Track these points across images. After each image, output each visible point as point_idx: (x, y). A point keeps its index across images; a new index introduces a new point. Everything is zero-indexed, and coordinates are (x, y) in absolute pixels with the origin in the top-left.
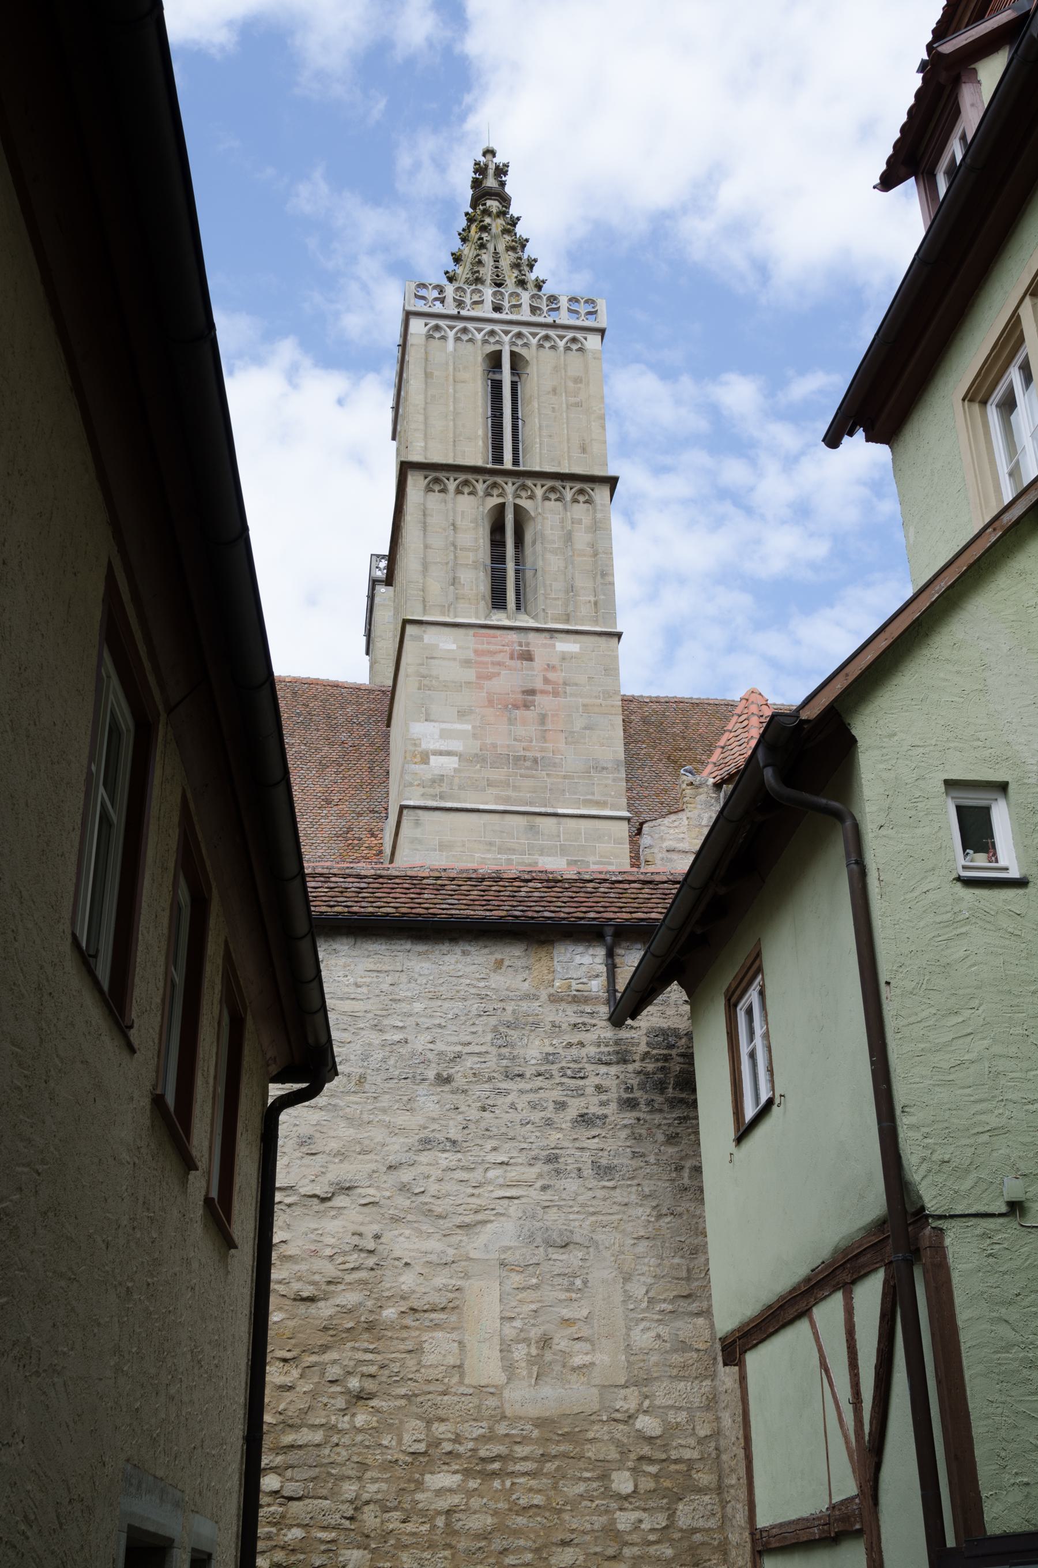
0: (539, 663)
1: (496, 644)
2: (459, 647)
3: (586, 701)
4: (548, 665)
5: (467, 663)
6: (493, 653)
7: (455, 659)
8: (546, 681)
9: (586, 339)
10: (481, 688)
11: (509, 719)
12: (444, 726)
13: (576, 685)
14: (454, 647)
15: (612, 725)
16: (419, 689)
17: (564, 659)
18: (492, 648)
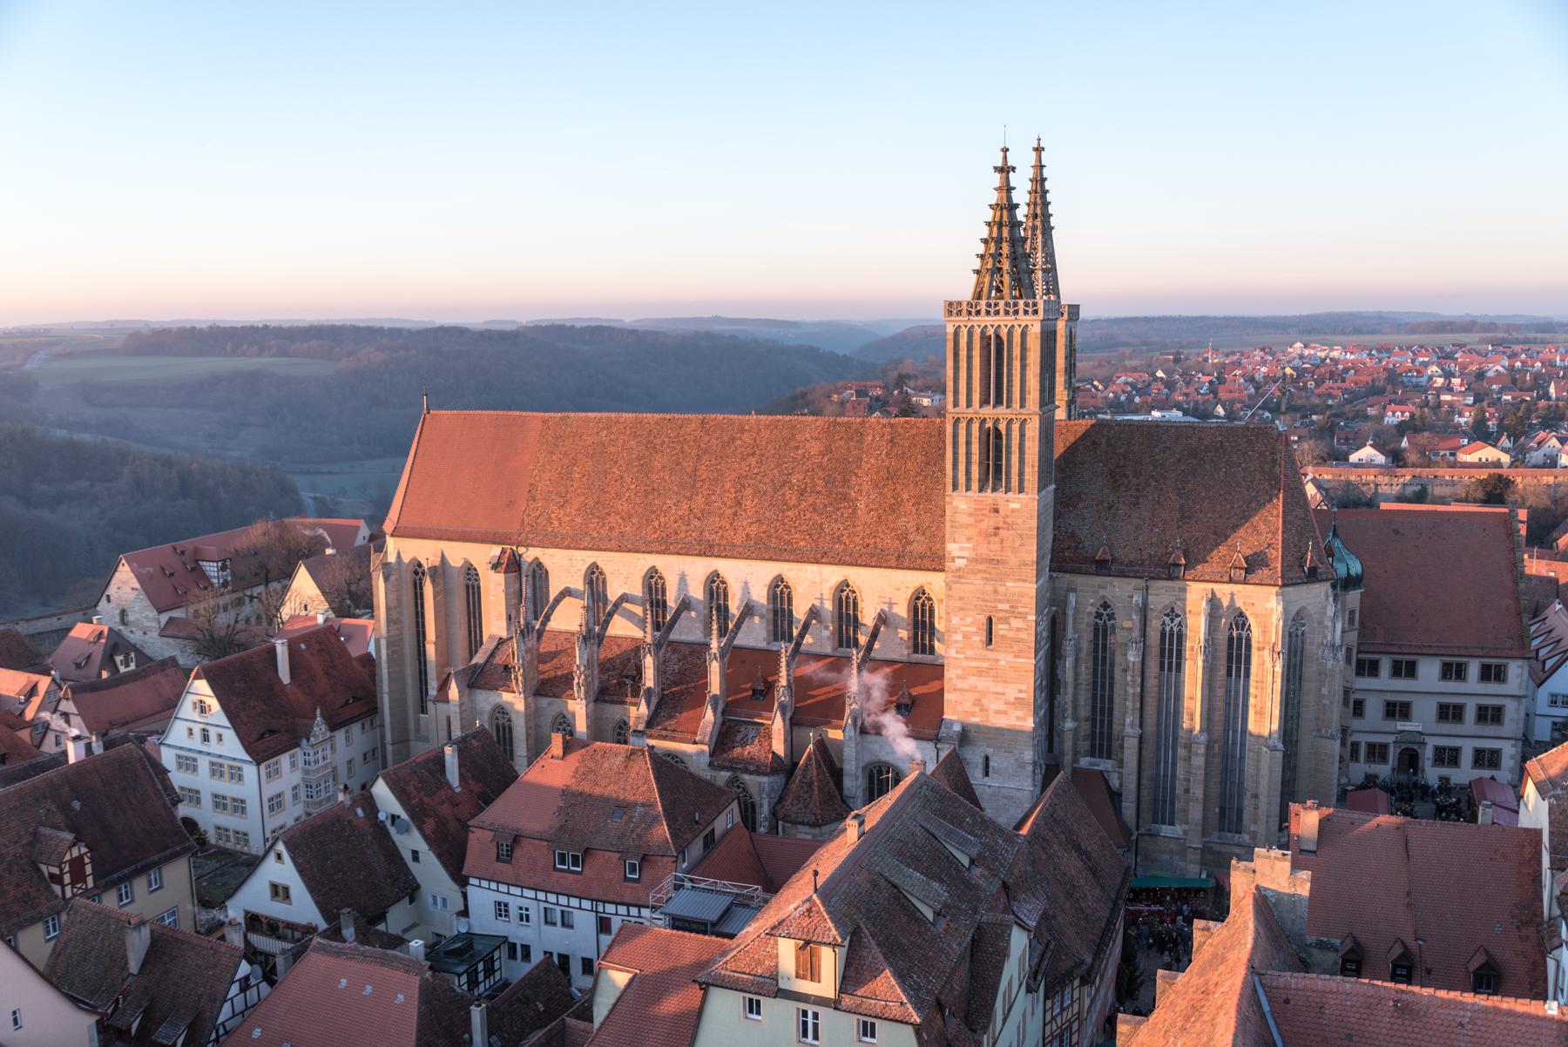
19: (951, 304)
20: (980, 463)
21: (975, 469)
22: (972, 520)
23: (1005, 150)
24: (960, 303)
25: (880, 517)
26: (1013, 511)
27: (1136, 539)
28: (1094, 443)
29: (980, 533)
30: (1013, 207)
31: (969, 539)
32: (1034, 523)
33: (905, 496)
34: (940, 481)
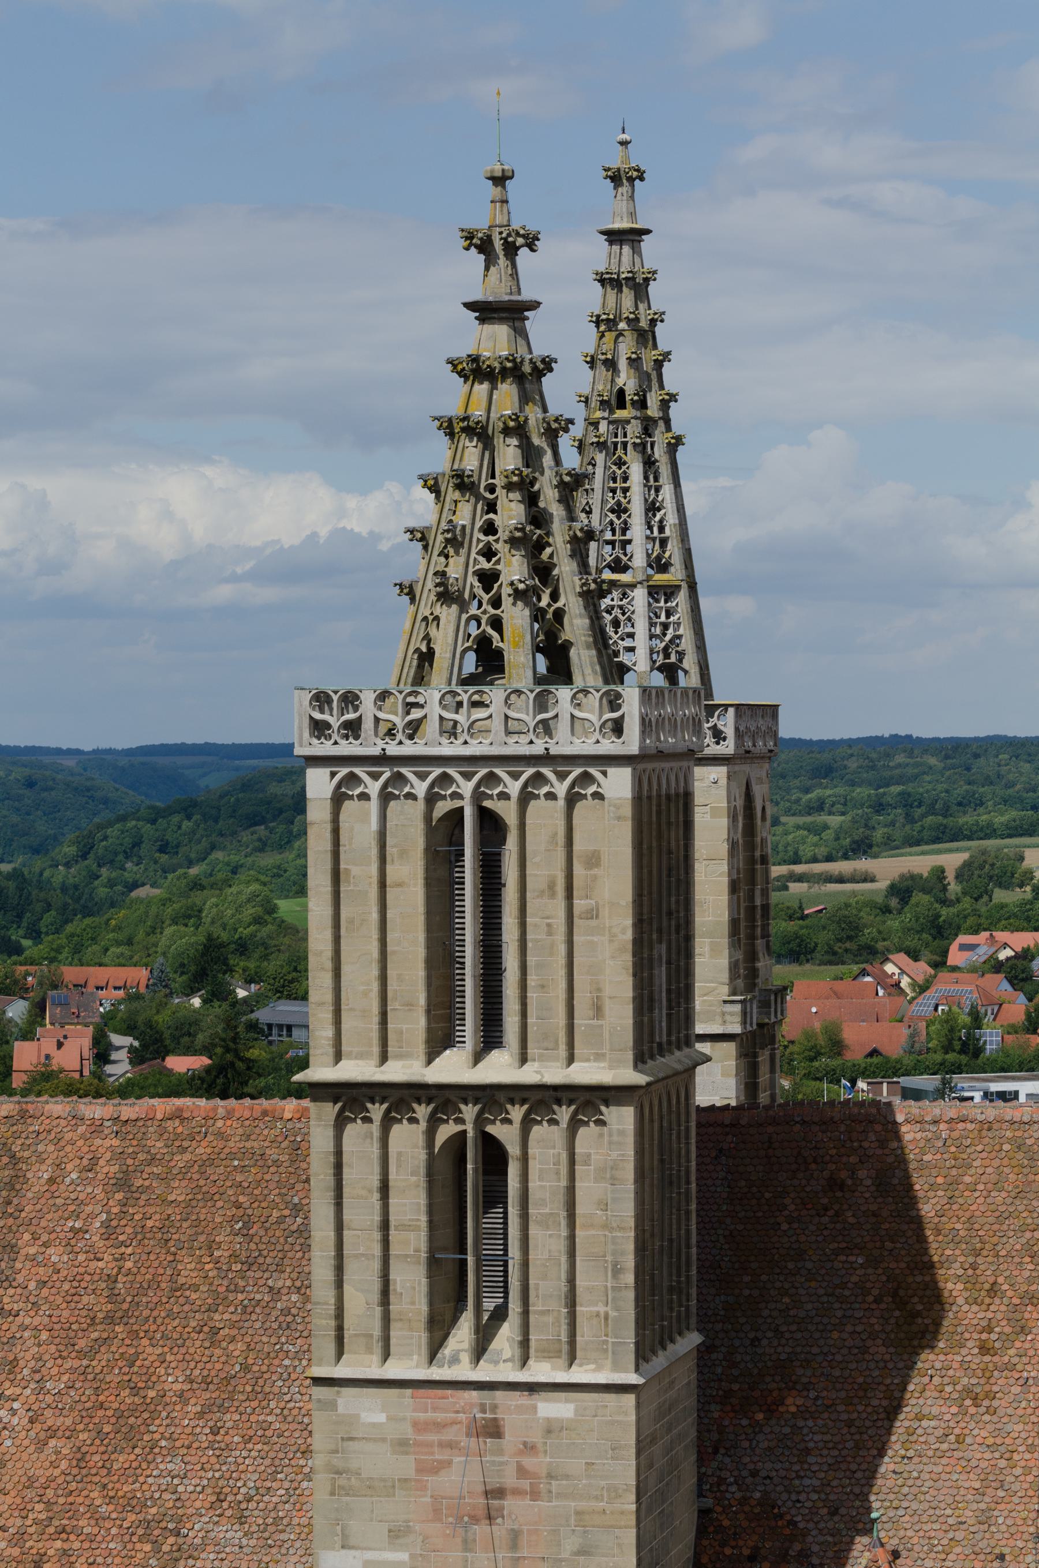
0: (511, 1439)
1: (446, 1411)
2: (388, 1418)
3: (583, 1505)
4: (525, 1444)
5: (402, 1445)
6: (439, 1426)
7: (383, 1440)
8: (522, 1472)
9: (605, 773)
10: (424, 1488)
11: (465, 1541)
12: (370, 1555)
13: (567, 1477)
14: (382, 1418)
15: (619, 1545)
16: (332, 1494)
17: (549, 1432)
18: (440, 1416)
19: (321, 699)
20: (433, 1263)
21: (412, 1284)
22: (406, 1466)
23: (500, 180)
24: (350, 699)
25: (81, 1459)
26: (551, 1428)
27: (985, 1520)
28: (834, 1184)
29: (437, 1513)
30: (528, 375)
31: (396, 1535)
32: (624, 1472)
33: (173, 1382)
34: (293, 1324)
